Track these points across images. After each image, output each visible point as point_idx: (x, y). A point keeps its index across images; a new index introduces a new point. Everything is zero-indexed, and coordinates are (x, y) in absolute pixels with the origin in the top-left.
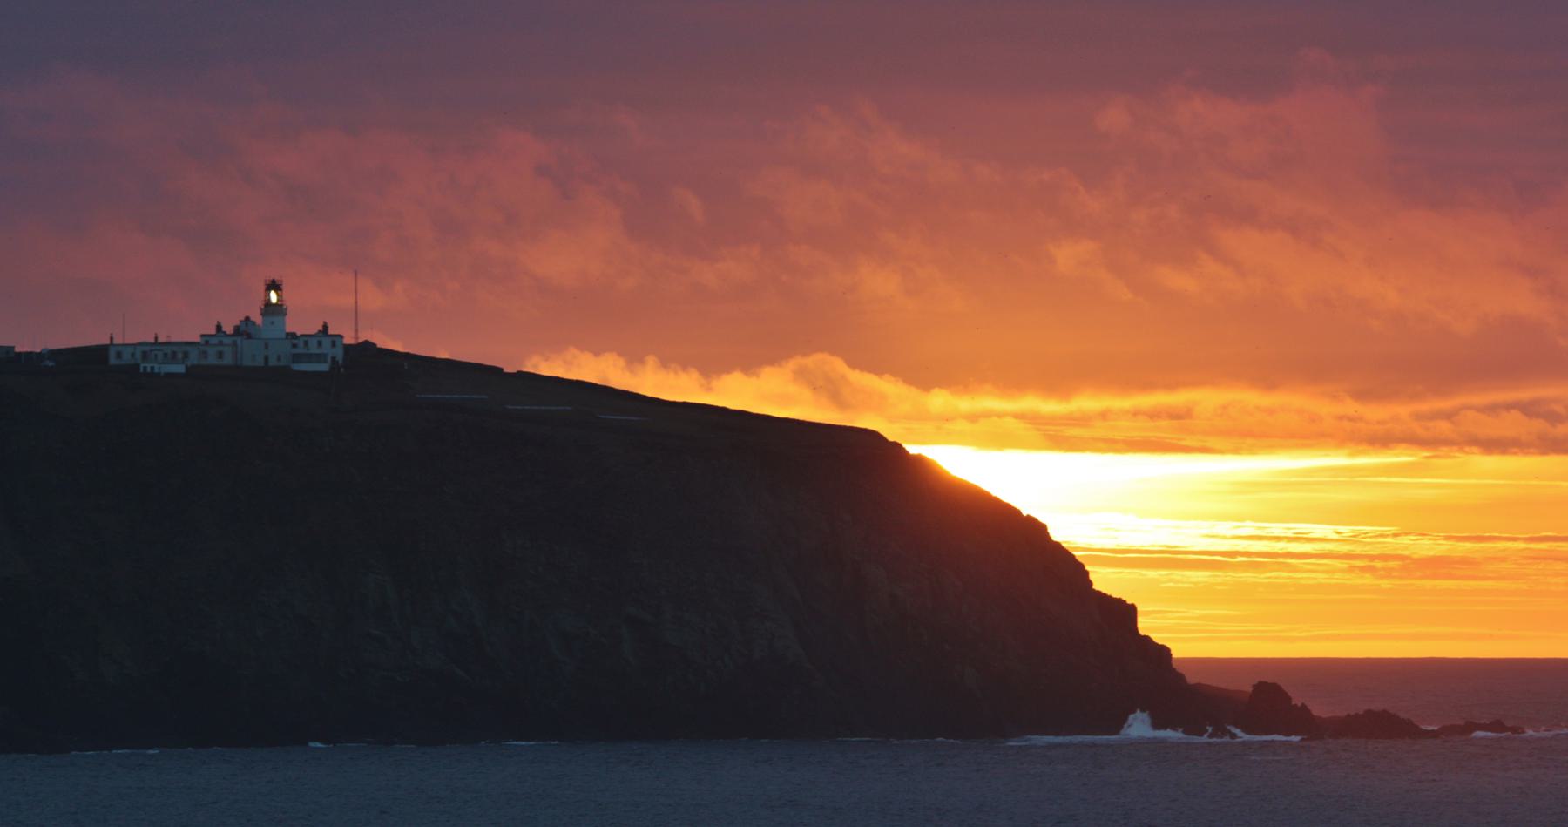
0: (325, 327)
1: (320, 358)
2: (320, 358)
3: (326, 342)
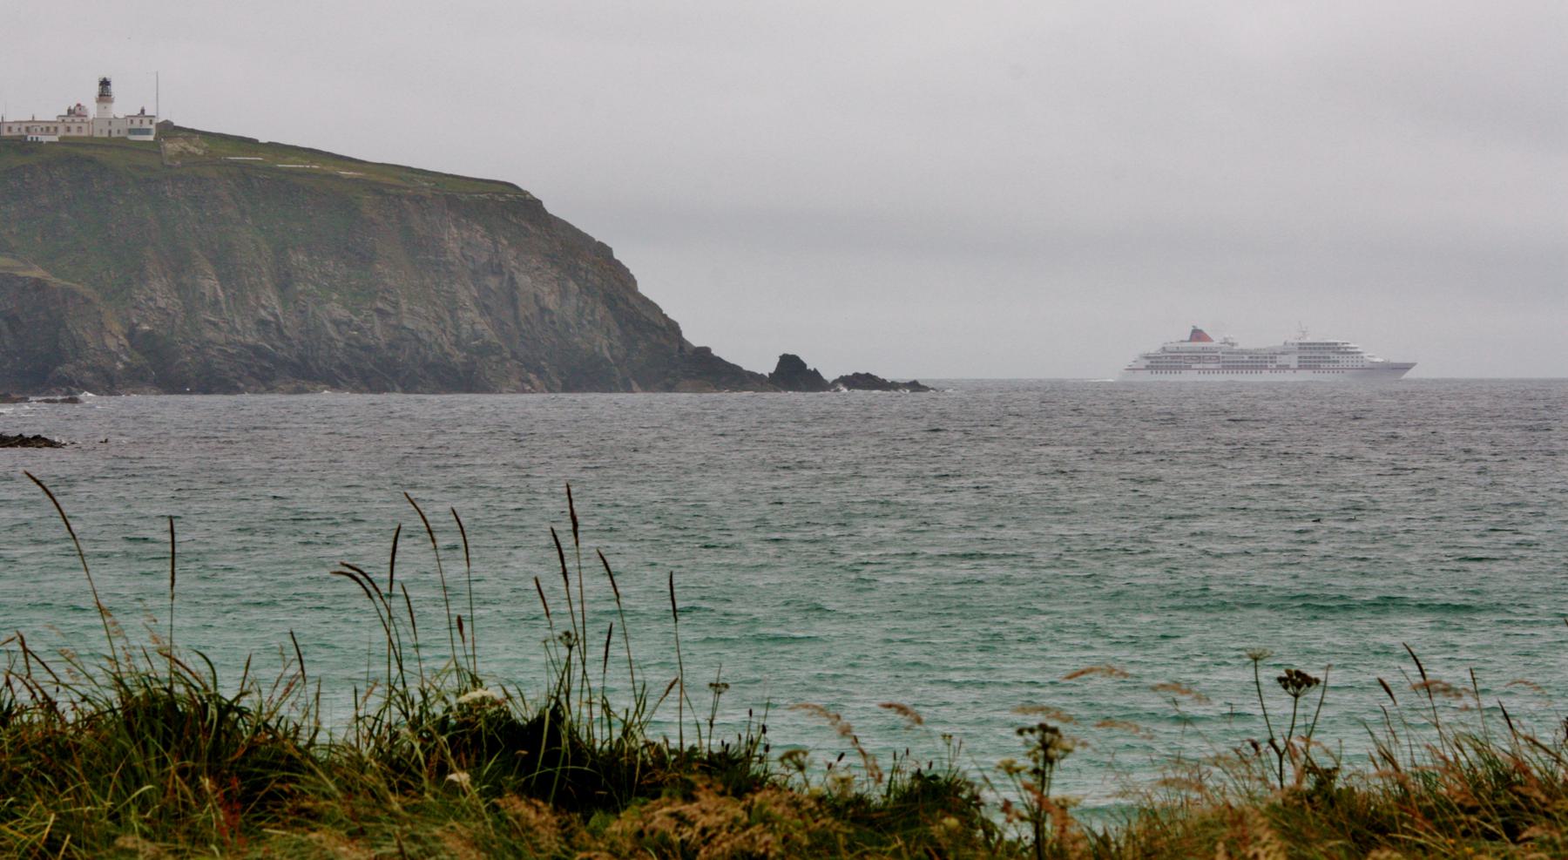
0: (143, 111)
1: (147, 132)
2: (147, 132)
3: (146, 121)
